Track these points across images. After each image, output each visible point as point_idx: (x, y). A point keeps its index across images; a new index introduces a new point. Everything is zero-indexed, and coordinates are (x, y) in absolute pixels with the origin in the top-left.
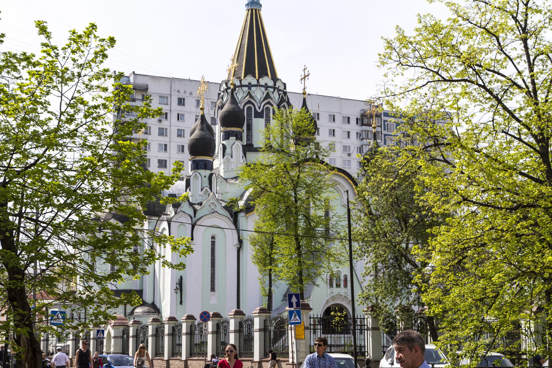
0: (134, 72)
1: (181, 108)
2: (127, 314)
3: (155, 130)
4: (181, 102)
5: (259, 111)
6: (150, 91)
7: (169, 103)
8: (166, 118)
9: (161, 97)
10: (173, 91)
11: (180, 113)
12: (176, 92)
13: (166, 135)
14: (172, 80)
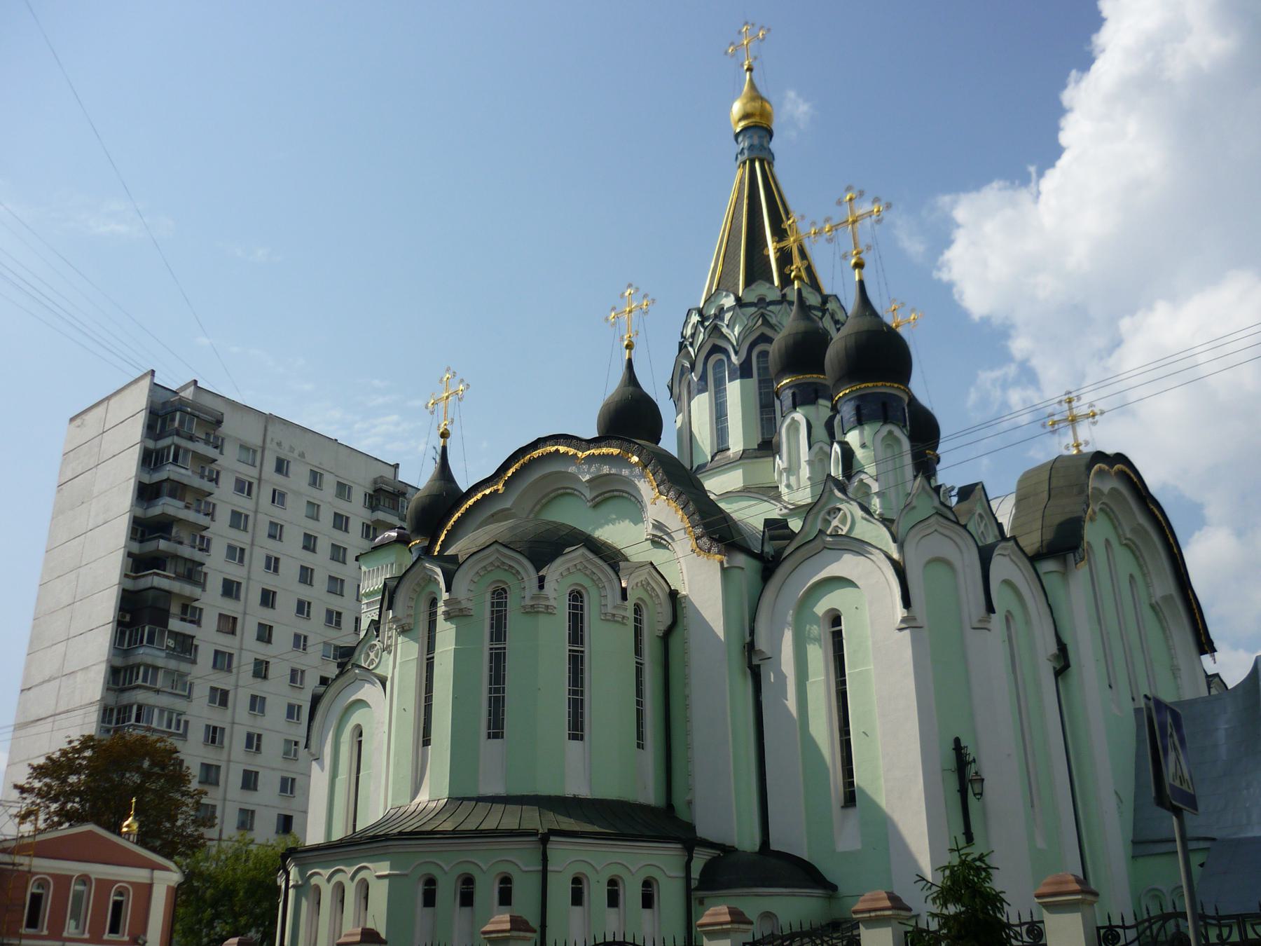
0: (195, 382)
1: (279, 478)
2: (694, 884)
3: (223, 515)
4: (281, 466)
6: (227, 428)
7: (258, 463)
9: (244, 447)
10: (268, 440)
11: (275, 487)
12: (274, 444)
13: (245, 530)
14: (270, 419)
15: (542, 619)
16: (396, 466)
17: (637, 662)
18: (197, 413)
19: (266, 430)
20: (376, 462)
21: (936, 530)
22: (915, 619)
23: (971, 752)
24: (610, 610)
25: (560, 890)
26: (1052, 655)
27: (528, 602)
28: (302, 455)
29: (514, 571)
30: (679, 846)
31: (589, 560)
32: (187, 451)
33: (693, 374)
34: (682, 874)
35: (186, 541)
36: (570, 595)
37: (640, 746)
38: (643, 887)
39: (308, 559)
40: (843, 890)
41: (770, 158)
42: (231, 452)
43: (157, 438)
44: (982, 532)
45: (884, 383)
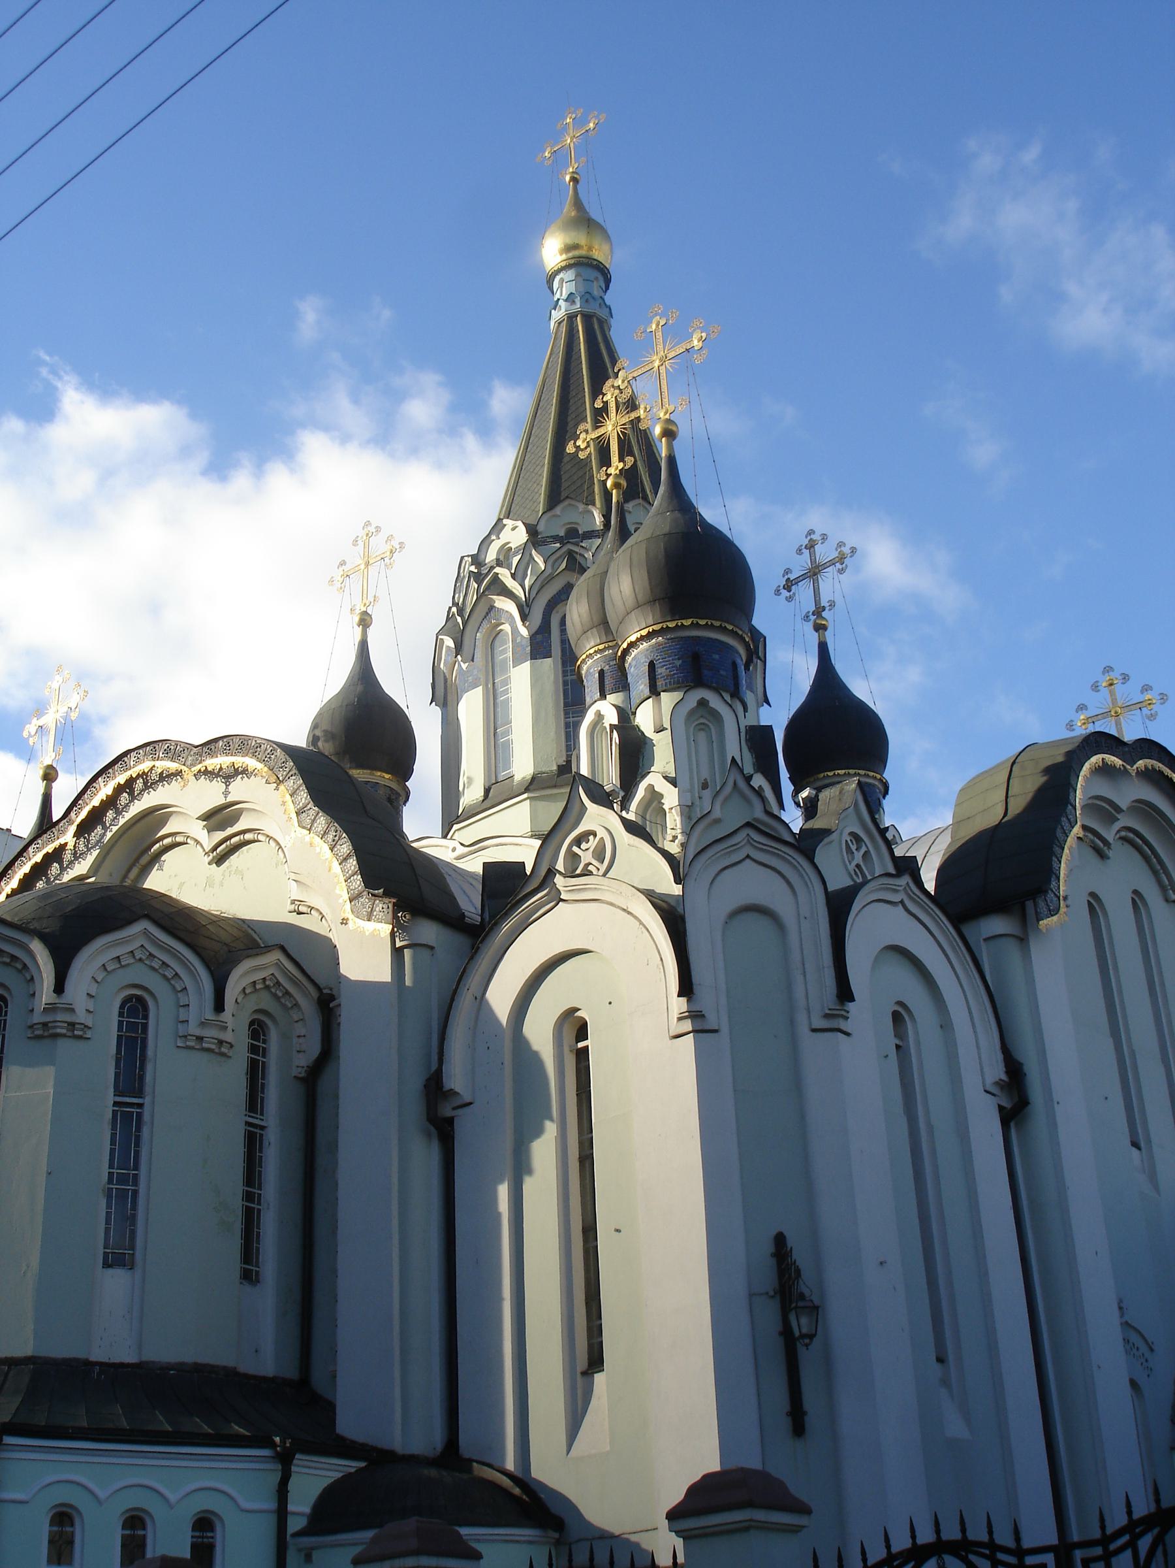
2: (295, 1524)
17: (248, 1124)
21: (748, 856)
22: (703, 1016)
23: (801, 1256)
24: (193, 1029)
26: (996, 1083)
27: (37, 1018)
29: (19, 966)
30: (266, 1452)
33: (459, 657)
34: (273, 1505)
36: (122, 1007)
37: (249, 1276)
38: (194, 1529)
41: (603, 313)
44: (858, 866)
45: (695, 621)
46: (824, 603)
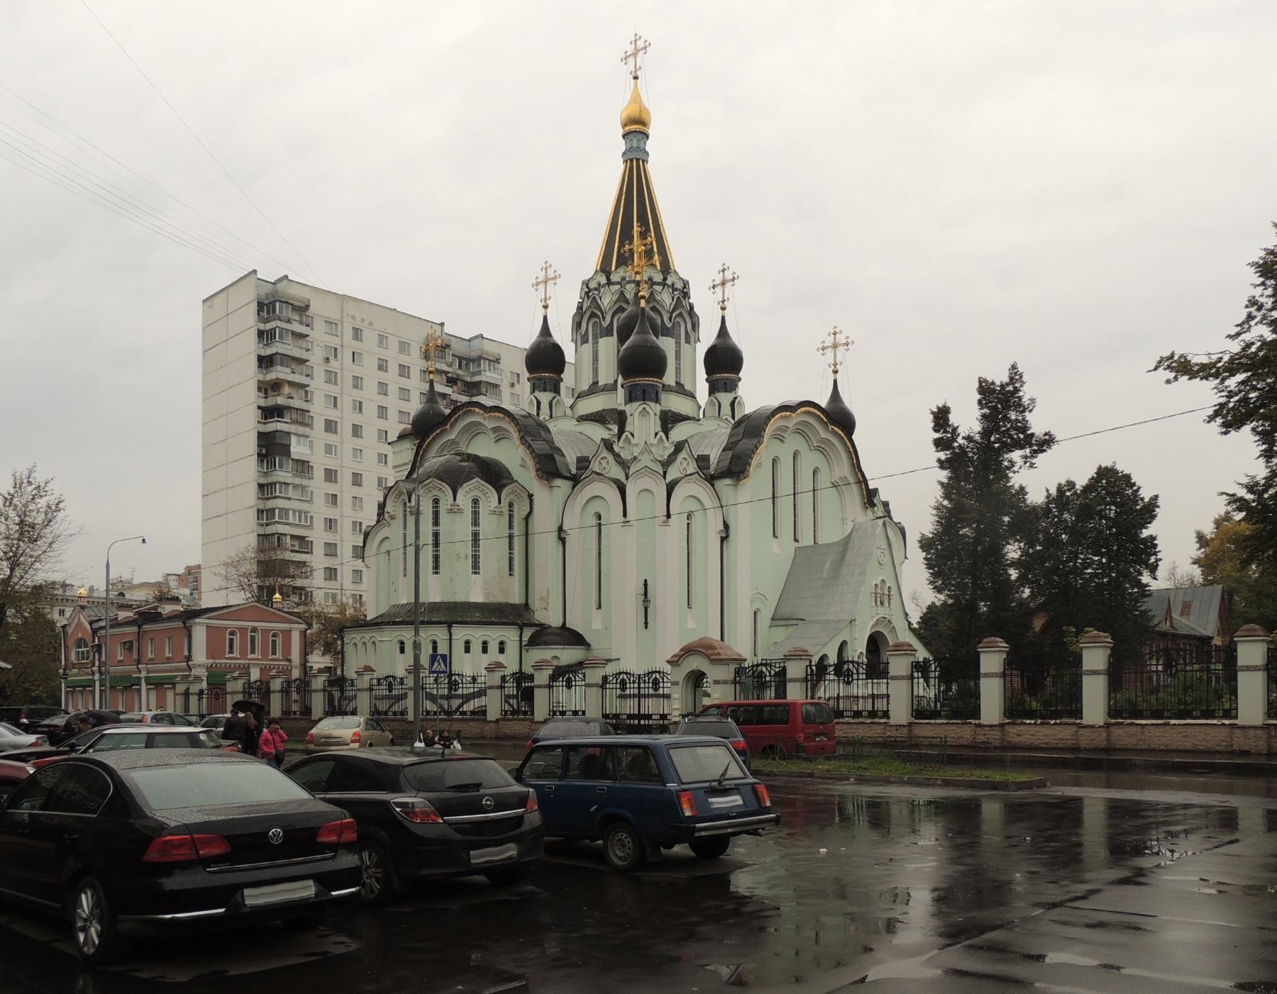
2: (524, 644)
4: (357, 334)
5: (669, 325)
7: (339, 334)
8: (336, 357)
10: (345, 314)
12: (350, 318)
13: (336, 383)
14: (344, 298)
15: (457, 516)
16: (442, 324)
18: (291, 302)
19: (342, 307)
20: (426, 323)
25: (458, 647)
28: (371, 324)
31: (482, 485)
32: (287, 330)
35: (295, 397)
39: (383, 401)
40: (593, 645)
42: (319, 325)
43: (266, 321)
46: (726, 298)
